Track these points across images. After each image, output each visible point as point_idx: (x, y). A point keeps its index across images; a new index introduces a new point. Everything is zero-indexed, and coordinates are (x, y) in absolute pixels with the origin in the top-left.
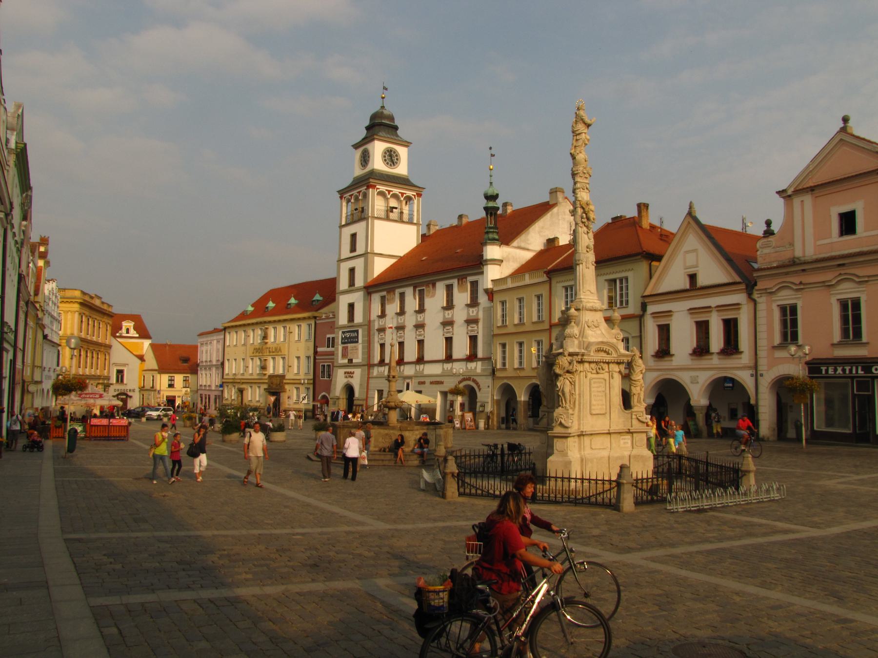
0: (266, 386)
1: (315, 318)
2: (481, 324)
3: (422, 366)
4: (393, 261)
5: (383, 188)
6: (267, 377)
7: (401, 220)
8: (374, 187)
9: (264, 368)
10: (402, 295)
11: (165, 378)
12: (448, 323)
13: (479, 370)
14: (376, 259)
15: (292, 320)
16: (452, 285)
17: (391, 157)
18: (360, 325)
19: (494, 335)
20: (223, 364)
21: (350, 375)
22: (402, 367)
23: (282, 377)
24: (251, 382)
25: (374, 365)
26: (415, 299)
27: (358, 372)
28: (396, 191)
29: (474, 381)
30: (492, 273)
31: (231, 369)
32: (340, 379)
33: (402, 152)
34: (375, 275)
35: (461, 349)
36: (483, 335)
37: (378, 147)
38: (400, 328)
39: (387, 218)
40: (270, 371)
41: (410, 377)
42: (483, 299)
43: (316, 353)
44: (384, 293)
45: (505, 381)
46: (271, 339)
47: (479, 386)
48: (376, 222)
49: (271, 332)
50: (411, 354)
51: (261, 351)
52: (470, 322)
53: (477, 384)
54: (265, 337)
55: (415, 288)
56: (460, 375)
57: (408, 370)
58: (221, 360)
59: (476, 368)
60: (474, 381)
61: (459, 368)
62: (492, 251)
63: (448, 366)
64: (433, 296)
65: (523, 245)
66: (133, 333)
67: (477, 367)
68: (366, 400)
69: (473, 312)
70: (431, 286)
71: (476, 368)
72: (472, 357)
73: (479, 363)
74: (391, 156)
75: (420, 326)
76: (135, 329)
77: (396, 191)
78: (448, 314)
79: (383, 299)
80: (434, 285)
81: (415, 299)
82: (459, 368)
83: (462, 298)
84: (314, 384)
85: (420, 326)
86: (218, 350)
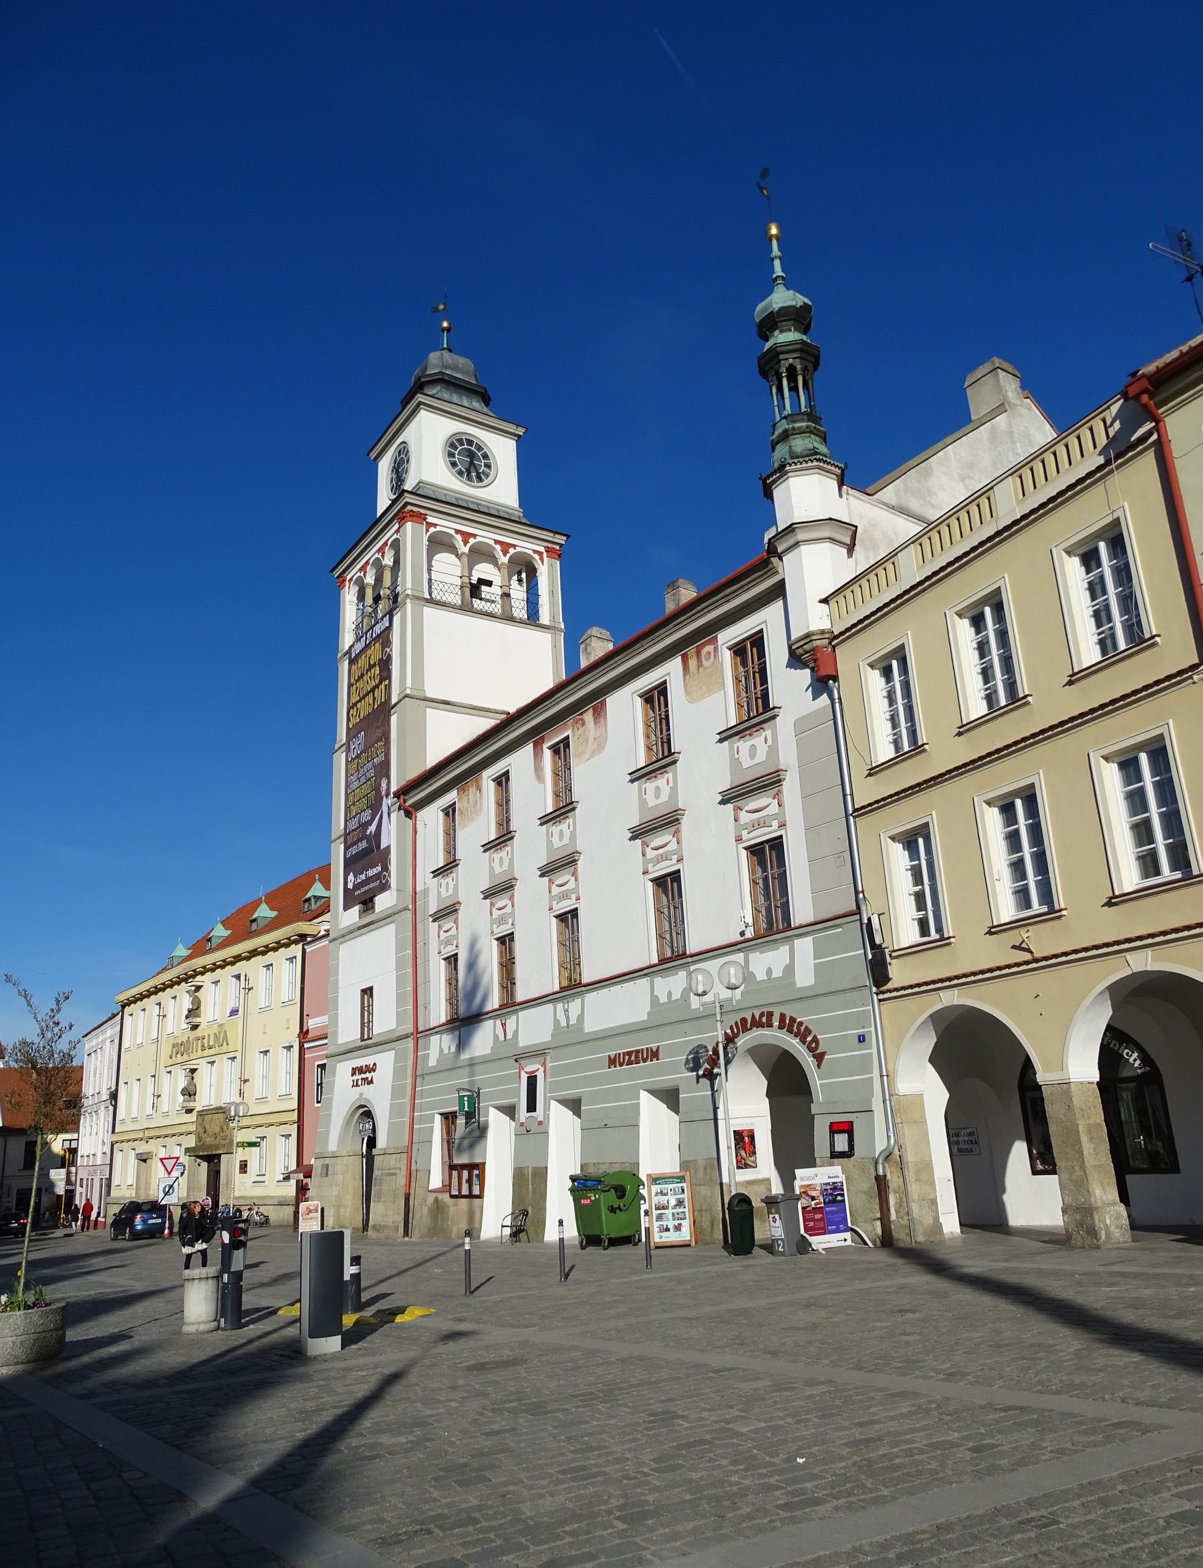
0: (191, 1142)
1: (302, 937)
2: (791, 787)
3: (575, 1006)
4: (485, 724)
5: (446, 525)
6: (193, 1117)
7: (509, 618)
8: (420, 518)
9: (189, 1093)
10: (503, 780)
13: (805, 977)
14: (433, 715)
15: (254, 953)
16: (663, 688)
18: (388, 917)
19: (860, 812)
20: (114, 1096)
21: (364, 1074)
22: (511, 1022)
24: (164, 1134)
25: (432, 1031)
26: (540, 778)
27: (385, 1062)
28: (486, 536)
29: (789, 1025)
31: (132, 1105)
32: (343, 1091)
34: (431, 761)
35: (720, 902)
36: (809, 828)
38: (501, 889)
39: (466, 608)
40: (204, 1100)
41: (538, 1053)
42: (789, 687)
43: (304, 1034)
44: (451, 796)
45: (951, 998)
47: (813, 1047)
48: (429, 612)
49: (209, 995)
50: (538, 971)
53: (803, 1034)
54: (193, 1012)
55: (538, 746)
56: (725, 1008)
57: (533, 1028)
58: (114, 1088)
59: (790, 969)
60: (789, 1025)
61: (716, 983)
63: (672, 985)
64: (600, 745)
65: (915, 505)
67: (798, 962)
68: (409, 1150)
69: (753, 753)
70: (589, 717)
71: (790, 969)
73: (805, 946)
74: (471, 455)
77: (486, 536)
78: (657, 793)
79: (450, 811)
80: (599, 712)
81: (540, 778)
84: (300, 1122)
86: (111, 1061)
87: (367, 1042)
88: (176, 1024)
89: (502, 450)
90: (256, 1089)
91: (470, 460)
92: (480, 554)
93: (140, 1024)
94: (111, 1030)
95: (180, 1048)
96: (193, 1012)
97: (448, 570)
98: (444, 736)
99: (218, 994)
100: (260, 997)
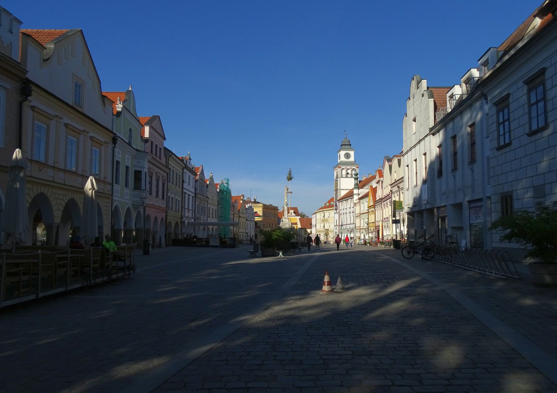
4: (348, 191)
8: (340, 167)
9: (324, 227)
11: (303, 231)
12: (350, 213)
17: (347, 156)
23: (328, 230)
30: (356, 197)
33: (352, 153)
37: (342, 153)
39: (347, 177)
40: (326, 228)
46: (326, 217)
49: (326, 214)
51: (324, 220)
52: (353, 212)
54: (324, 216)
61: (352, 226)
62: (356, 191)
66: (293, 214)
67: (354, 225)
72: (354, 223)
75: (346, 213)
76: (294, 213)
82: (348, 226)
83: (352, 205)
85: (346, 213)
87: (336, 225)
88: (322, 217)
89: (352, 153)
90: (331, 227)
91: (347, 156)
92: (349, 169)
93: (318, 215)
94: (315, 215)
95: (323, 221)
96: (324, 216)
97: (344, 172)
98: (343, 193)
99: (327, 214)
100: (331, 216)
